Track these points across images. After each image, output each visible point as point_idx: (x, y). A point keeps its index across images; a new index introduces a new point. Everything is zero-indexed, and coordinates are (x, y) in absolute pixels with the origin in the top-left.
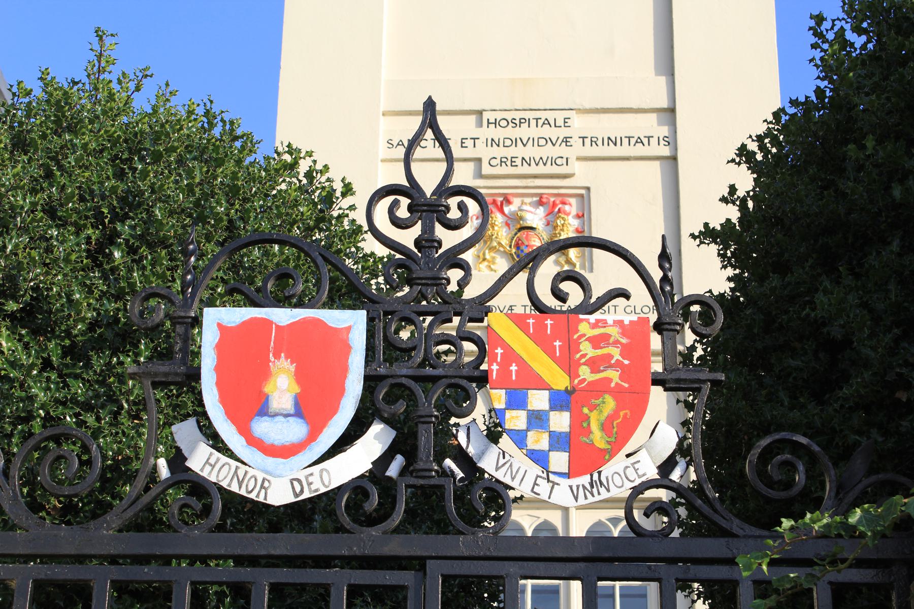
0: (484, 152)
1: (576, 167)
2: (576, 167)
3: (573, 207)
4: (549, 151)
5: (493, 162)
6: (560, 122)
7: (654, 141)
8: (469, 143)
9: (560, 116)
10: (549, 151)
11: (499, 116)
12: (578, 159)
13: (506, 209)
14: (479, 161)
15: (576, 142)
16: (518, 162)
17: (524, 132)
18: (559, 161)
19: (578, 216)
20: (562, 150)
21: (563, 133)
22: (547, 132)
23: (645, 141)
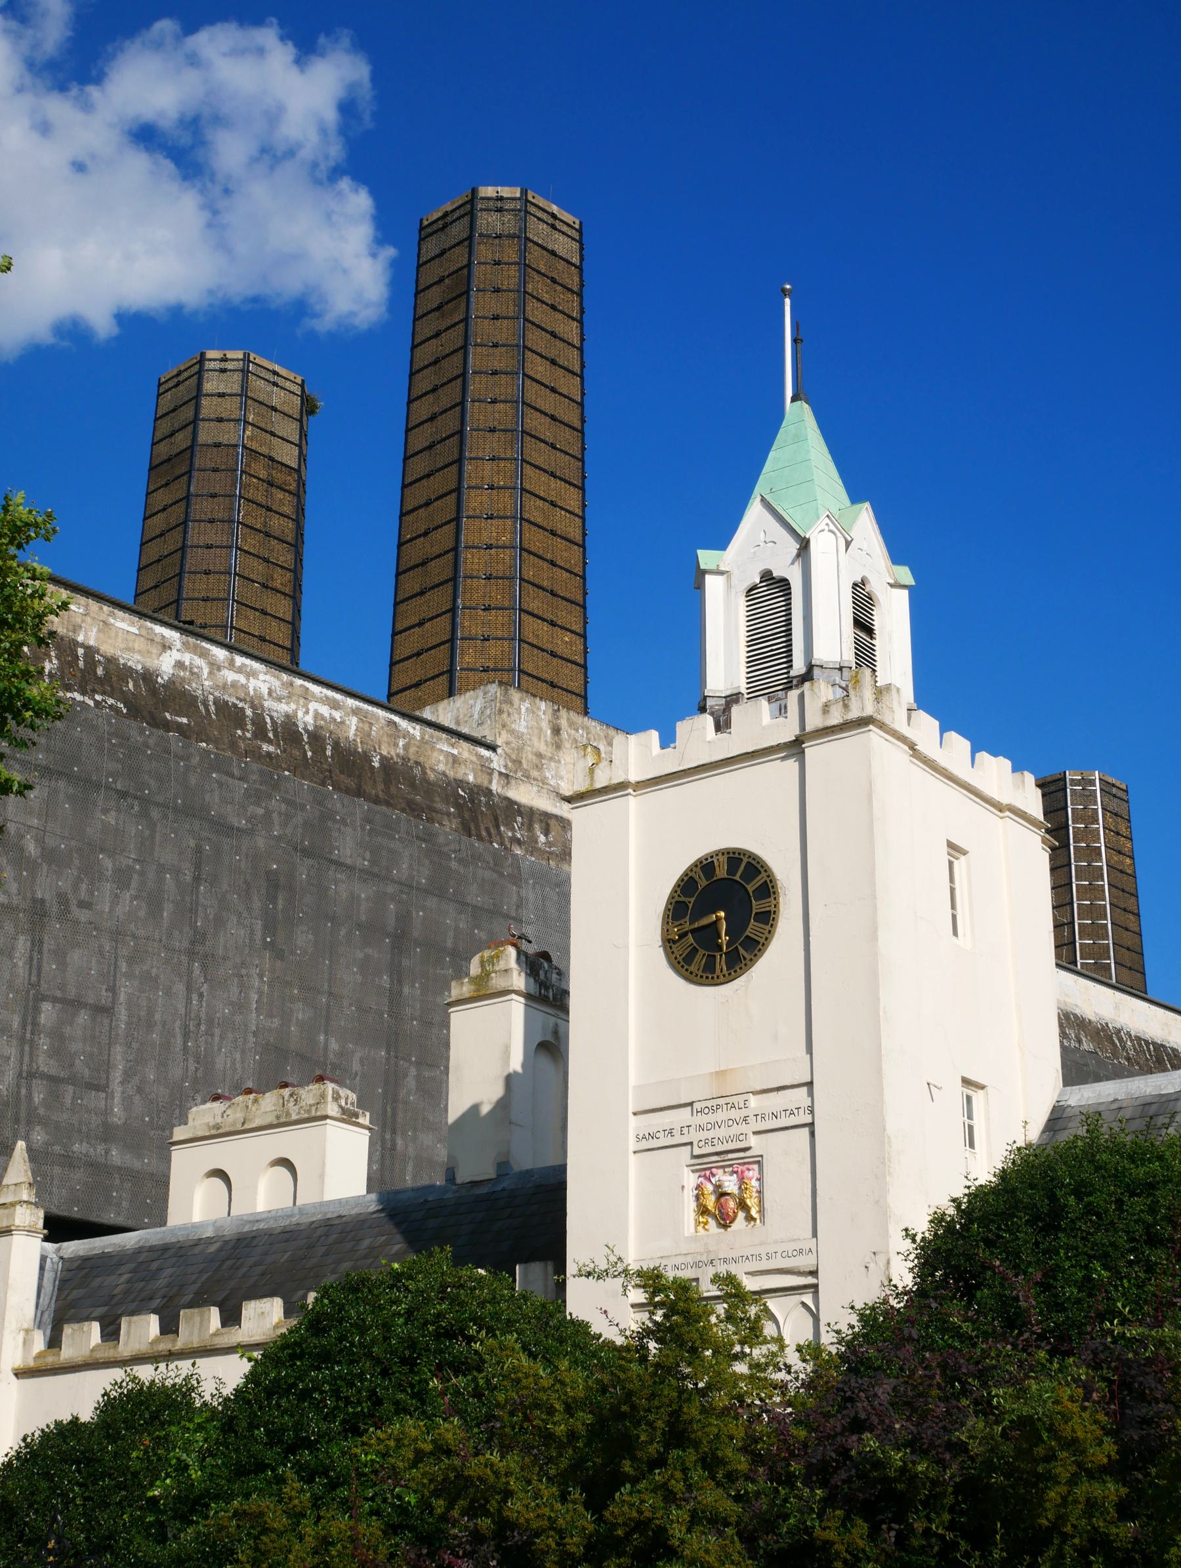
0: (694, 1136)
1: (753, 1141)
2: (753, 1141)
3: (753, 1173)
4: (735, 1130)
5: (701, 1144)
6: (742, 1105)
7: (801, 1111)
8: (685, 1130)
9: (741, 1098)
10: (735, 1130)
11: (703, 1105)
12: (754, 1133)
13: (713, 1180)
14: (691, 1144)
15: (752, 1119)
16: (716, 1141)
17: (721, 1116)
18: (741, 1138)
19: (759, 1180)
20: (743, 1128)
21: (744, 1113)
22: (734, 1114)
23: (796, 1111)
